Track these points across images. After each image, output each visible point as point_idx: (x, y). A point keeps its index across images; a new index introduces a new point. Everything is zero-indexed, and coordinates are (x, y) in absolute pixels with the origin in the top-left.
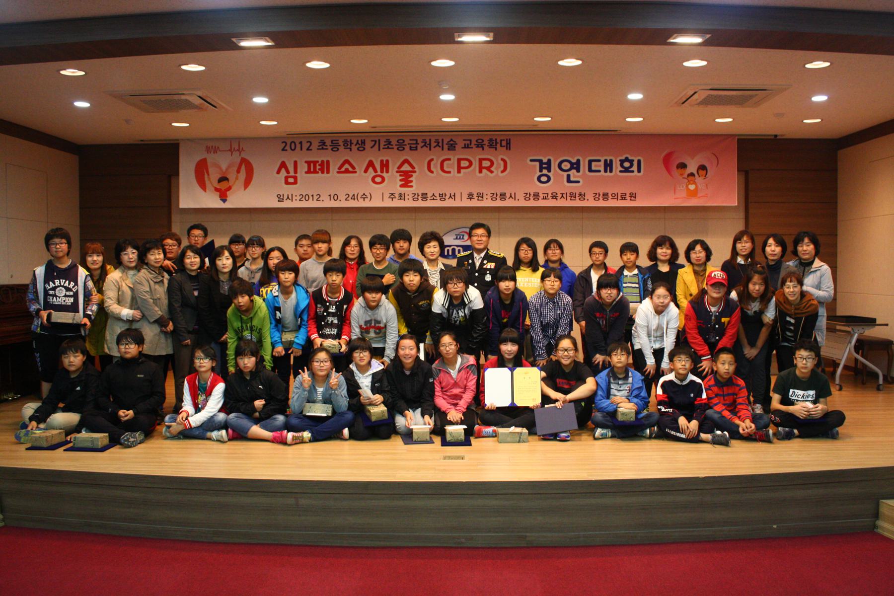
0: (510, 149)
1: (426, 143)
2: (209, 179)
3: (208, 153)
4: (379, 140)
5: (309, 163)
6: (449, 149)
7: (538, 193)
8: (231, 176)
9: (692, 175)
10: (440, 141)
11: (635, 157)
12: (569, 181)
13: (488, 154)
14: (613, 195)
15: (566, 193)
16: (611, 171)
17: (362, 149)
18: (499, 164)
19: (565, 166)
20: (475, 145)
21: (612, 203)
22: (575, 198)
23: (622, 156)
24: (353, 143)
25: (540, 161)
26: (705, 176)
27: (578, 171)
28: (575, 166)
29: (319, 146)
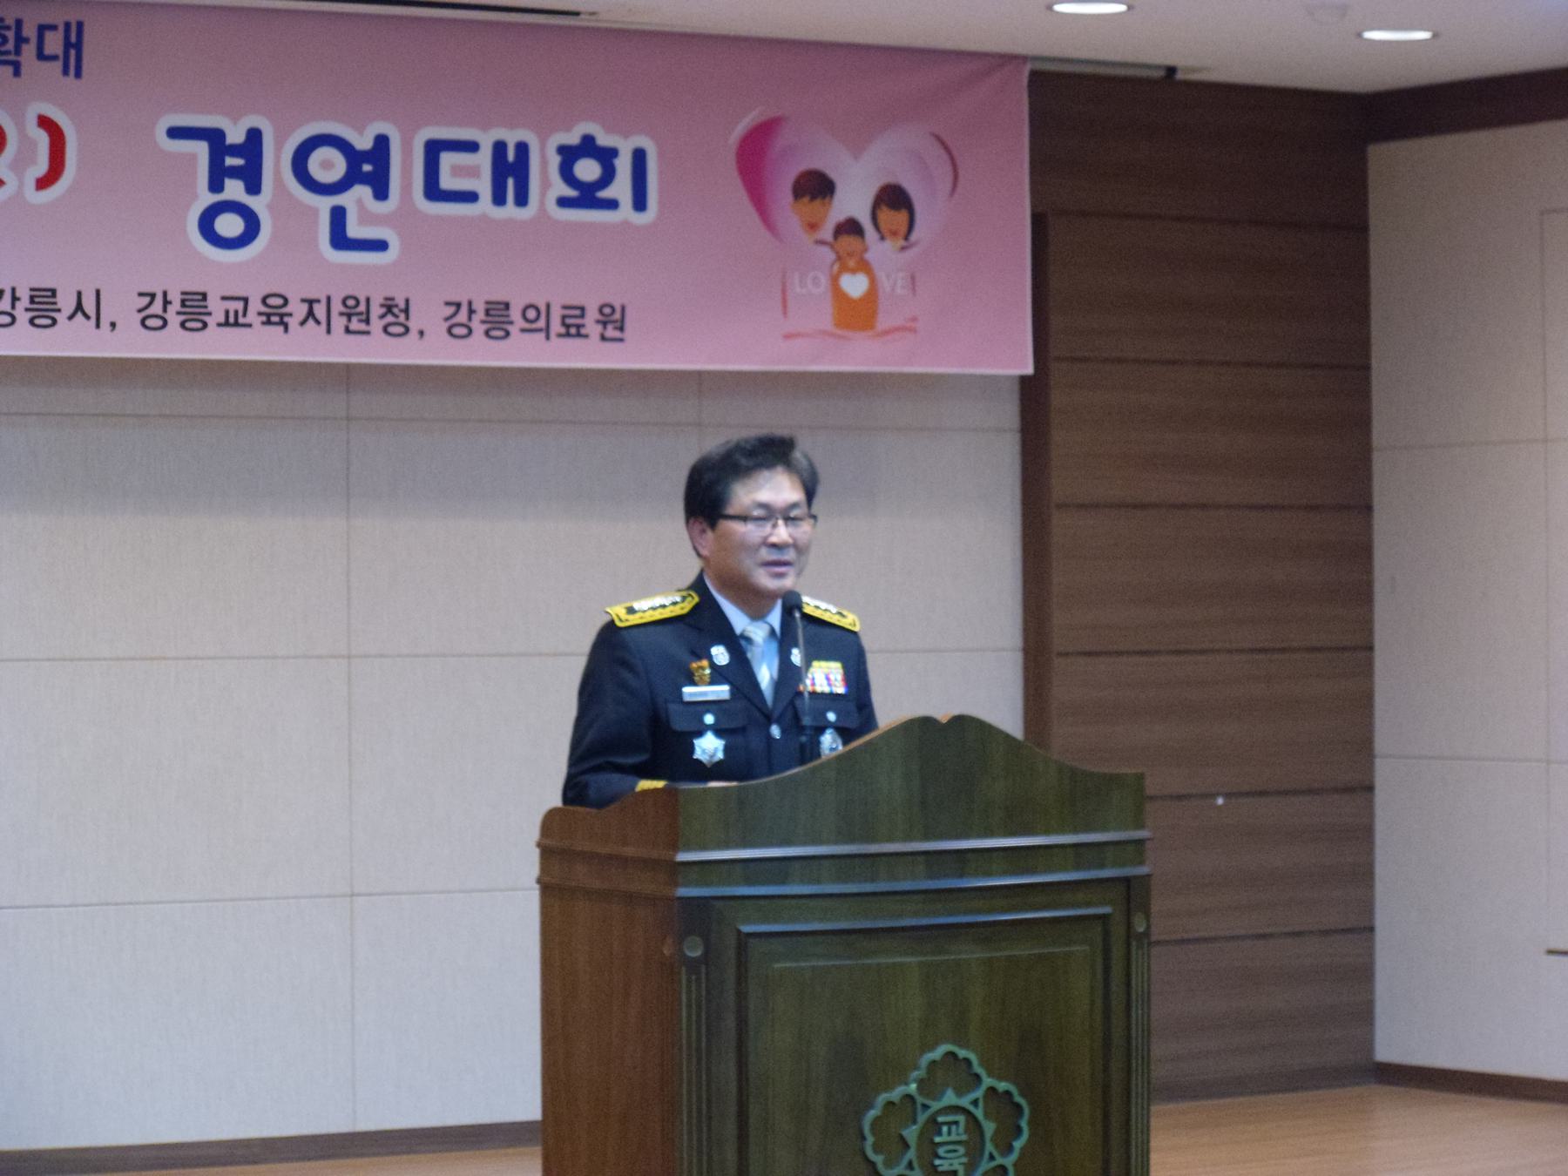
0: (78, 74)
7: (204, 296)
9: (850, 228)
11: (626, 135)
12: (340, 240)
14: (531, 314)
15: (329, 299)
16: (522, 200)
18: (27, 144)
19: (328, 165)
22: (367, 321)
23: (568, 129)
25: (214, 137)
26: (906, 238)
27: (381, 193)
28: (367, 168)
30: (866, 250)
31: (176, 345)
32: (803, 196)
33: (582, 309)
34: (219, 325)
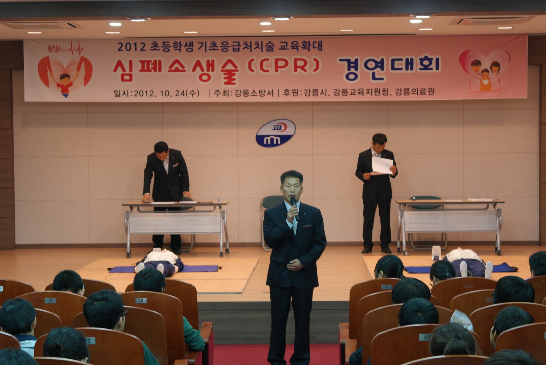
0: (321, 50)
1: (247, 45)
2: (52, 76)
3: (50, 52)
4: (206, 43)
5: (142, 62)
6: (267, 51)
7: (347, 90)
8: (72, 73)
9: (486, 71)
10: (260, 43)
12: (374, 78)
13: (302, 54)
15: (372, 89)
16: (412, 69)
17: (190, 50)
19: (371, 65)
20: (291, 46)
21: (412, 97)
22: (380, 93)
24: (182, 45)
25: (349, 61)
26: (498, 72)
27: (382, 69)
28: (379, 65)
29: (152, 47)
30: (489, 75)
31: (341, 98)
32: (474, 65)
33: (425, 89)
34: (350, 95)
